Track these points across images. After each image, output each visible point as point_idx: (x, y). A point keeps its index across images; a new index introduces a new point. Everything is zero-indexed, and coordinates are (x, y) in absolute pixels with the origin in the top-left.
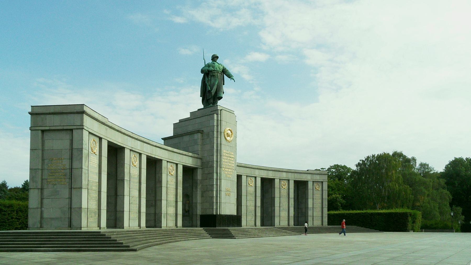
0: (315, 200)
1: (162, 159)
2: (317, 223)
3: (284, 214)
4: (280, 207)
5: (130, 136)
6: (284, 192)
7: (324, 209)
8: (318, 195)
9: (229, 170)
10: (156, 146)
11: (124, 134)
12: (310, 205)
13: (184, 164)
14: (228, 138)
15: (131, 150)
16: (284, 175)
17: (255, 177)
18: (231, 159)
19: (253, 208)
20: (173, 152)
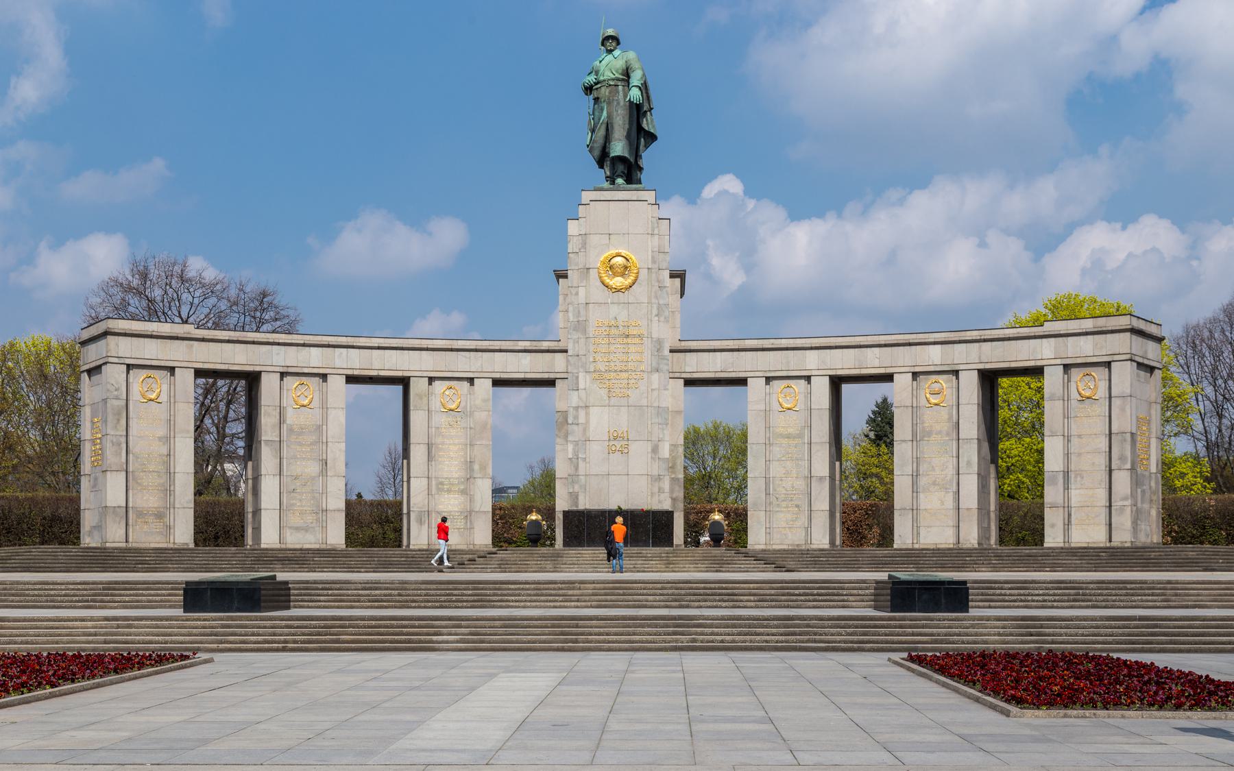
0: (1075, 440)
1: (406, 374)
2: (1089, 534)
3: (935, 502)
4: (915, 476)
5: (279, 344)
6: (936, 420)
7: (1115, 474)
8: (1090, 424)
9: (625, 375)
10: (379, 348)
11: (254, 343)
12: (1053, 461)
13: (497, 376)
14: (618, 282)
15: (283, 375)
16: (934, 356)
17: (808, 379)
18: (629, 340)
19: (801, 484)
20: (452, 350)
